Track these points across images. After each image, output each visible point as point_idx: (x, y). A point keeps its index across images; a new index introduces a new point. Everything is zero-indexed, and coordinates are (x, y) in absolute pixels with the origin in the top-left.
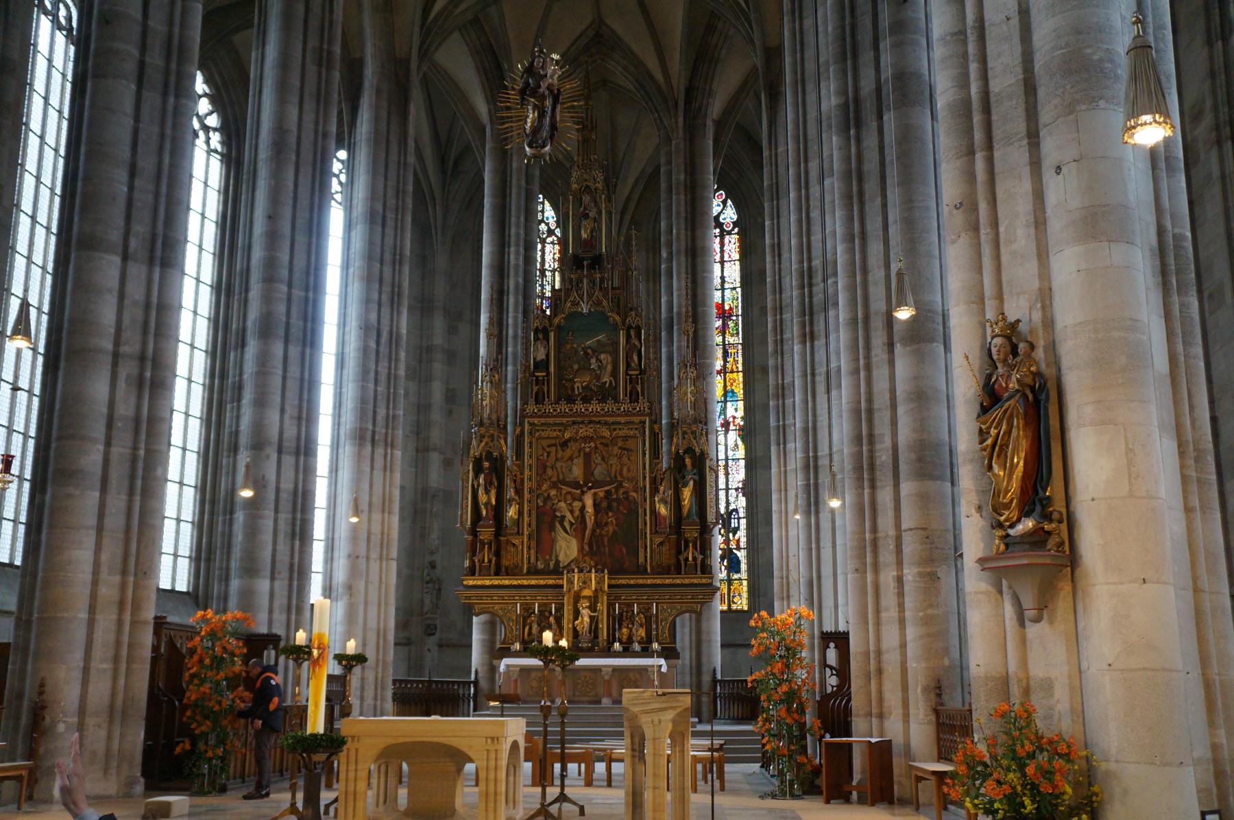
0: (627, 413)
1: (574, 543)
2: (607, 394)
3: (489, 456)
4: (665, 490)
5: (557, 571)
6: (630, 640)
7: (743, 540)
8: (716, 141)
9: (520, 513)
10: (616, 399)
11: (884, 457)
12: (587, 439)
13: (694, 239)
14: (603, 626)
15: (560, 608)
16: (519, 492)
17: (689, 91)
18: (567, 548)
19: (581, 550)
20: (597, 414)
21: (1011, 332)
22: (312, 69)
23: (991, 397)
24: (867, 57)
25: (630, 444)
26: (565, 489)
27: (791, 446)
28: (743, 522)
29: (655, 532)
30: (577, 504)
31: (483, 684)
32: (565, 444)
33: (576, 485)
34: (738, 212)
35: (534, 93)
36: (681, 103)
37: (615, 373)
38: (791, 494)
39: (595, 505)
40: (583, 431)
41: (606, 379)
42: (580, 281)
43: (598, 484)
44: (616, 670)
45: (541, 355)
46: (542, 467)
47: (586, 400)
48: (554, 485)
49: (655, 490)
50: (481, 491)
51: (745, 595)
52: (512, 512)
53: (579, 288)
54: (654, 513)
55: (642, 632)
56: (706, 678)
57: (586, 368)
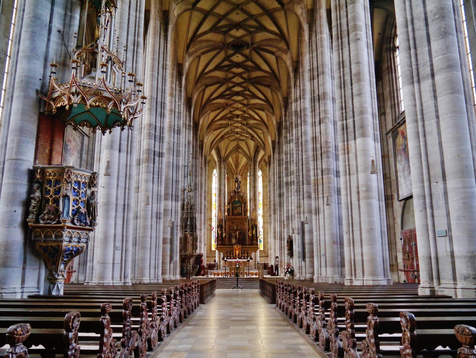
0: (244, 218)
1: (235, 240)
2: (241, 214)
3: (220, 225)
4: (250, 231)
5: (232, 245)
6: (244, 257)
7: (262, 238)
8: (259, 165)
9: (226, 235)
10: (242, 215)
11: (283, 238)
12: (237, 222)
13: (255, 185)
14: (240, 254)
15: (233, 251)
16: (225, 231)
17: (254, 157)
18: (234, 241)
19: (236, 241)
20: (238, 218)
21: (289, 236)
22: (200, 170)
23: (288, 242)
24: (282, 188)
25: (244, 223)
26: (233, 231)
27: (271, 225)
28: (262, 234)
29: (248, 238)
30: (235, 234)
31: (218, 264)
32: (233, 223)
33: (235, 230)
34: (262, 172)
35: (237, 182)
36: (253, 160)
37: (242, 211)
38: (272, 233)
39: (239, 234)
40: (237, 221)
41: (240, 211)
42: (236, 195)
43: (239, 230)
44: (243, 262)
45: (229, 208)
46: (229, 227)
47: (237, 215)
48: (231, 230)
49: (249, 231)
50: (219, 231)
51: (263, 247)
52: (224, 235)
53: (236, 196)
54: (248, 235)
55: (246, 255)
56: (257, 263)
57: (237, 210)
